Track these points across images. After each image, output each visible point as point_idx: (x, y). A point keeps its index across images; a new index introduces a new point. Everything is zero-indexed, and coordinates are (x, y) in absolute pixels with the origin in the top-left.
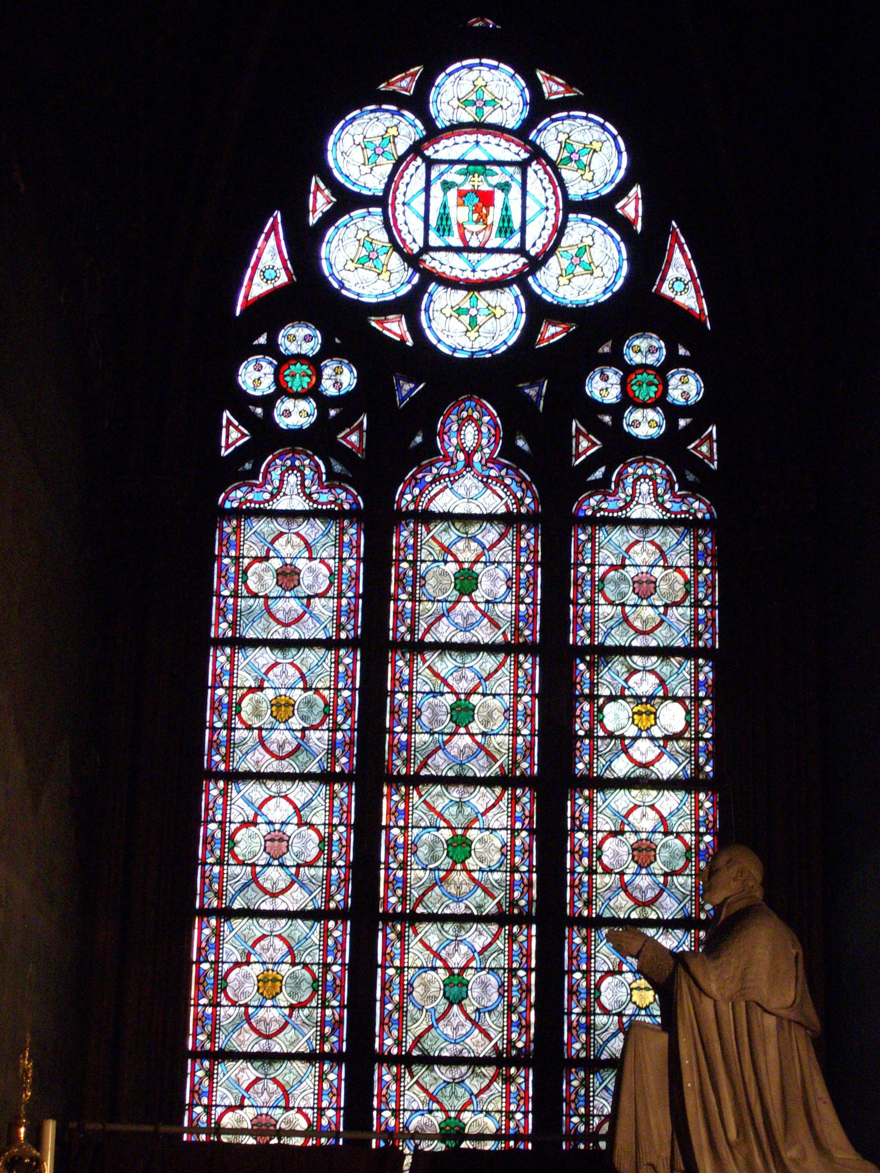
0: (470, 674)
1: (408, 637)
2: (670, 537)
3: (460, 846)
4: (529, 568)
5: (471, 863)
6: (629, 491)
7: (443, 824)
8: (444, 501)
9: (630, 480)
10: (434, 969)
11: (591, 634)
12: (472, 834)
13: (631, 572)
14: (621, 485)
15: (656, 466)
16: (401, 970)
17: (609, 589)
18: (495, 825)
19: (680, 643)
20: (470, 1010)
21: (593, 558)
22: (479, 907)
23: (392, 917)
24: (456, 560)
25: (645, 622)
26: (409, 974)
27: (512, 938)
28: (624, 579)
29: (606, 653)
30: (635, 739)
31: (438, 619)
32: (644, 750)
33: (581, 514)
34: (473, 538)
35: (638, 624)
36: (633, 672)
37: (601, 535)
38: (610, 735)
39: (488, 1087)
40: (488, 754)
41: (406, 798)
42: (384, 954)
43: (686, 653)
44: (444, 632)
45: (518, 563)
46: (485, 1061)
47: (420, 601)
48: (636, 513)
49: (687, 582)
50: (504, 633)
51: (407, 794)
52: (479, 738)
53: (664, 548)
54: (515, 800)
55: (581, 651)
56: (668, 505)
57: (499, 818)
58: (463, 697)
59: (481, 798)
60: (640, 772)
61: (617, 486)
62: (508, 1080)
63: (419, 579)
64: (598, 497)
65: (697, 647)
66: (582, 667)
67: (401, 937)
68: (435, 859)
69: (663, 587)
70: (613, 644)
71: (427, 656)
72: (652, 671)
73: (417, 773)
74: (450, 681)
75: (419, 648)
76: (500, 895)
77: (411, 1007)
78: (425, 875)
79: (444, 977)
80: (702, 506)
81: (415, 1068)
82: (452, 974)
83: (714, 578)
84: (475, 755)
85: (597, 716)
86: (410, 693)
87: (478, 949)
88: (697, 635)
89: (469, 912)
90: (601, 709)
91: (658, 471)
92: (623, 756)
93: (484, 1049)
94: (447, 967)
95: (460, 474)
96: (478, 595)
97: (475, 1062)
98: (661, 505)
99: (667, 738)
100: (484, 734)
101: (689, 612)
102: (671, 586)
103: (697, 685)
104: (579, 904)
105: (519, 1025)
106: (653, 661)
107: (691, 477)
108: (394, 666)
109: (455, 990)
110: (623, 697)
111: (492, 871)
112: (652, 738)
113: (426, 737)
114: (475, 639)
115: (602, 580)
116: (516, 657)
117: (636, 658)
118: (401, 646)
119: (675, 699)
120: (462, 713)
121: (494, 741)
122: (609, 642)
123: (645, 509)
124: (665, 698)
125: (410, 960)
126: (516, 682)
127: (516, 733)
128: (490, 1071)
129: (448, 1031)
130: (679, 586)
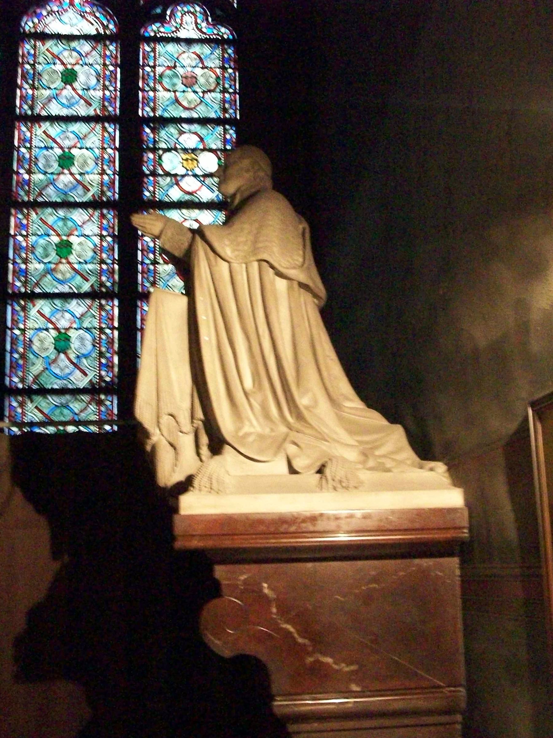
0: (72, 136)
1: (29, 112)
2: (206, 50)
3: (64, 247)
4: (111, 68)
5: (72, 258)
6: (178, 20)
7: (53, 233)
8: (54, 26)
9: (179, 14)
10: (47, 330)
11: (154, 110)
12: (72, 239)
13: (181, 71)
14: (173, 17)
15: (196, 6)
16: (23, 331)
17: (166, 82)
18: (89, 234)
19: (213, 115)
20: (72, 356)
21: (155, 63)
22: (79, 287)
23: (17, 296)
24: (63, 63)
25: (189, 102)
26: (29, 334)
27: (101, 308)
28: (176, 75)
29: (164, 122)
30: (183, 176)
31: (50, 101)
32: (190, 184)
33: (146, 35)
34: (74, 50)
35: (185, 104)
36: (181, 133)
37: (159, 48)
38: (167, 174)
39: (85, 409)
40: (85, 187)
41: (27, 216)
42: (13, 320)
43: (217, 122)
44: (55, 109)
45: (105, 65)
46: (83, 391)
47: (37, 89)
48: (182, 34)
49: (218, 77)
50: (95, 110)
51: (28, 214)
52: (78, 177)
53: (202, 56)
54: (103, 216)
55: (147, 121)
56: (204, 30)
57: (92, 229)
58: (67, 150)
59: (79, 216)
60: (187, 197)
61: (170, 17)
62: (100, 403)
63: (37, 75)
64: (158, 25)
65: (225, 118)
66: (147, 130)
67: (24, 309)
68: (47, 256)
69: (202, 80)
70: (169, 116)
71: (42, 124)
72: (196, 133)
73: (35, 200)
74: (58, 140)
75: (37, 119)
76: (93, 279)
77: (31, 356)
78: (41, 267)
79: (54, 336)
80: (228, 31)
81: (34, 397)
82: (60, 332)
83: (235, 75)
84: (74, 188)
85: (158, 161)
86: (30, 148)
87: (78, 316)
88: (225, 110)
89: (72, 291)
90: (160, 157)
91: (198, 9)
92: (175, 186)
93: (82, 382)
94: (56, 329)
95: (66, 11)
96: (76, 85)
97: (76, 392)
98: (200, 30)
99: (205, 176)
100: (81, 174)
101: (219, 96)
102: (207, 81)
103: (225, 141)
104: (147, 284)
105: (107, 366)
106: (196, 127)
107: (219, 12)
108: (20, 130)
109: (62, 343)
110: (176, 149)
111: (86, 263)
112: (195, 176)
113: (41, 177)
114: (75, 114)
115: (161, 76)
116: (103, 124)
117: (184, 125)
118: (25, 118)
119: (211, 150)
120: (66, 160)
121: (87, 177)
122: (166, 115)
123: (188, 32)
124: (204, 150)
125: (30, 324)
126: (103, 141)
127: (103, 172)
128: (86, 398)
129: (57, 371)
130: (212, 80)
